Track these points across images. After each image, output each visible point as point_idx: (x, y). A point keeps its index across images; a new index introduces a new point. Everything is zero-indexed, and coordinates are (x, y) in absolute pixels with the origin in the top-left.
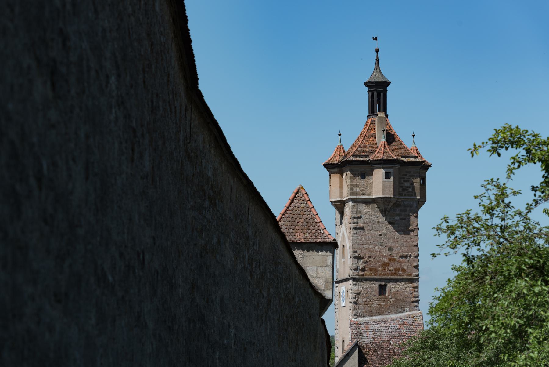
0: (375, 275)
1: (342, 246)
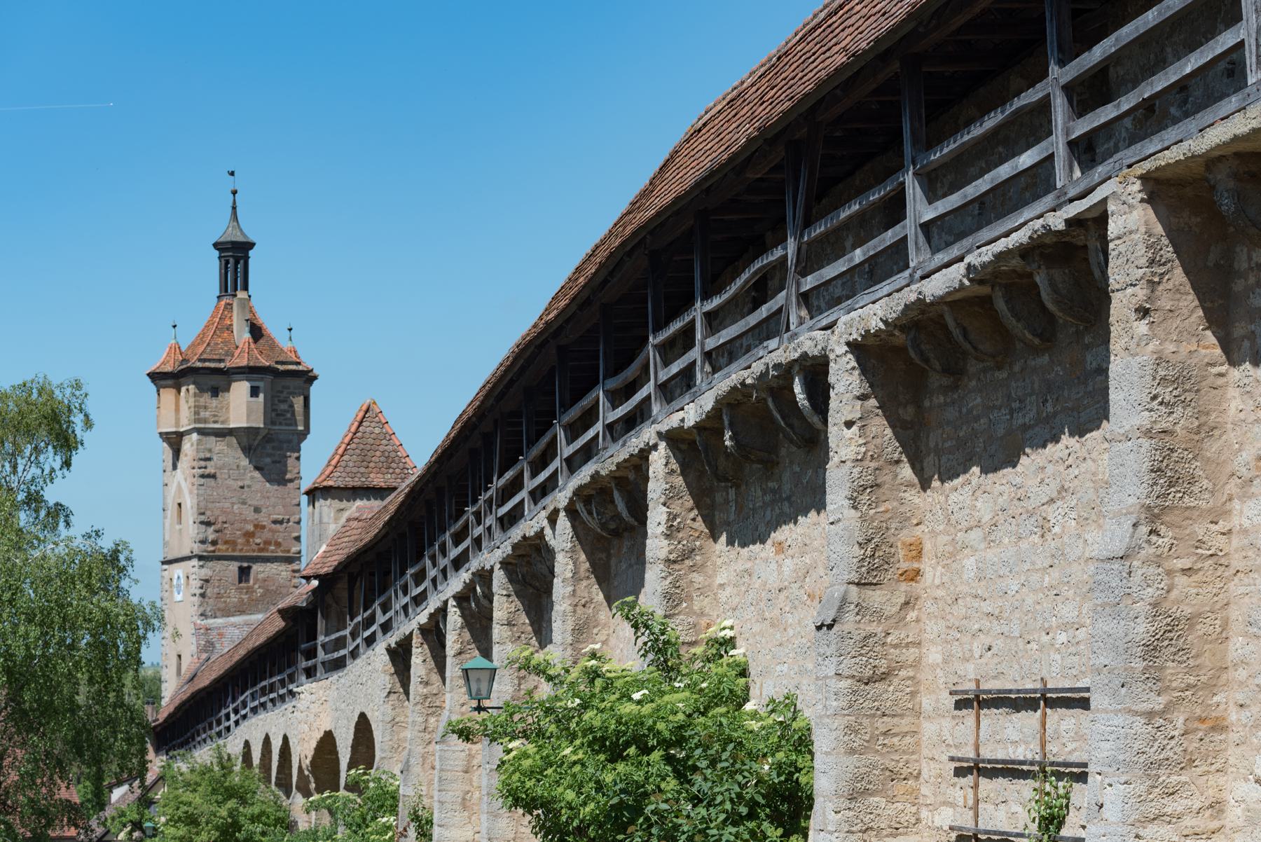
0: (234, 550)
1: (176, 506)
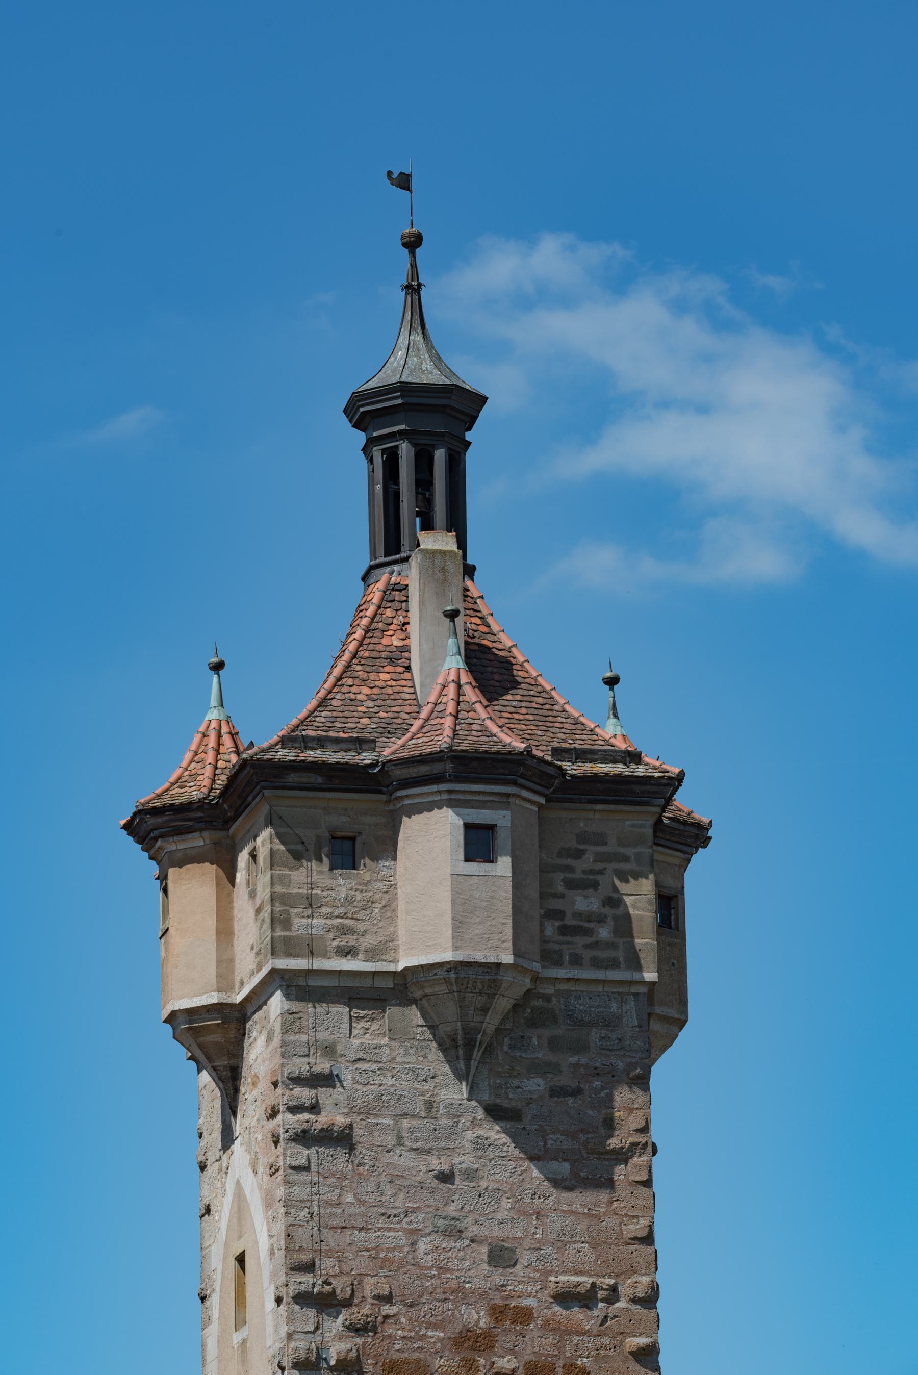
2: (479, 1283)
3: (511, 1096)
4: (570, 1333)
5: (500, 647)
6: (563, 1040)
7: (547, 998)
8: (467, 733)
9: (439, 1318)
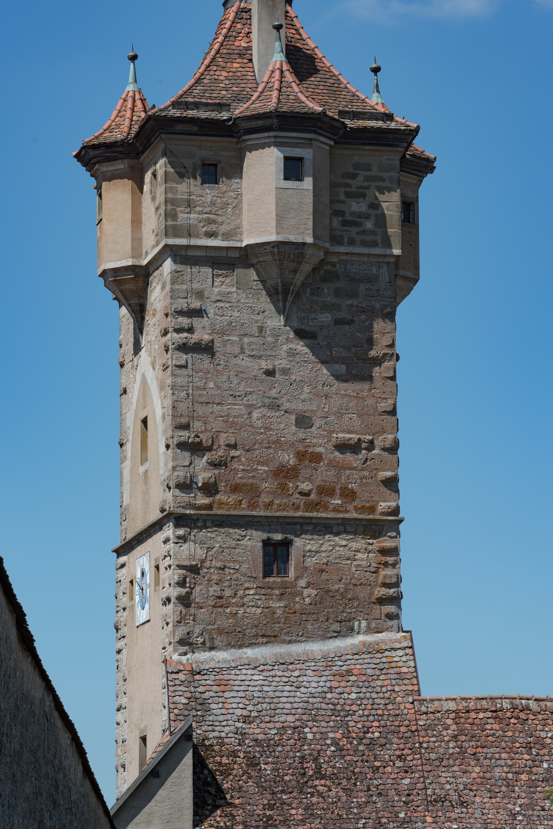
0: (253, 506)
2: (289, 437)
3: (311, 324)
4: (345, 469)
5: (308, 48)
6: (343, 290)
7: (334, 265)
8: (286, 101)
9: (265, 458)
